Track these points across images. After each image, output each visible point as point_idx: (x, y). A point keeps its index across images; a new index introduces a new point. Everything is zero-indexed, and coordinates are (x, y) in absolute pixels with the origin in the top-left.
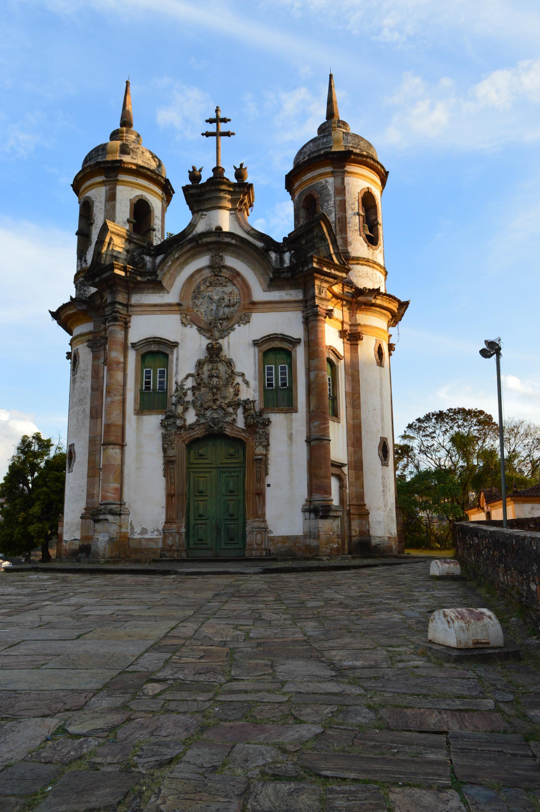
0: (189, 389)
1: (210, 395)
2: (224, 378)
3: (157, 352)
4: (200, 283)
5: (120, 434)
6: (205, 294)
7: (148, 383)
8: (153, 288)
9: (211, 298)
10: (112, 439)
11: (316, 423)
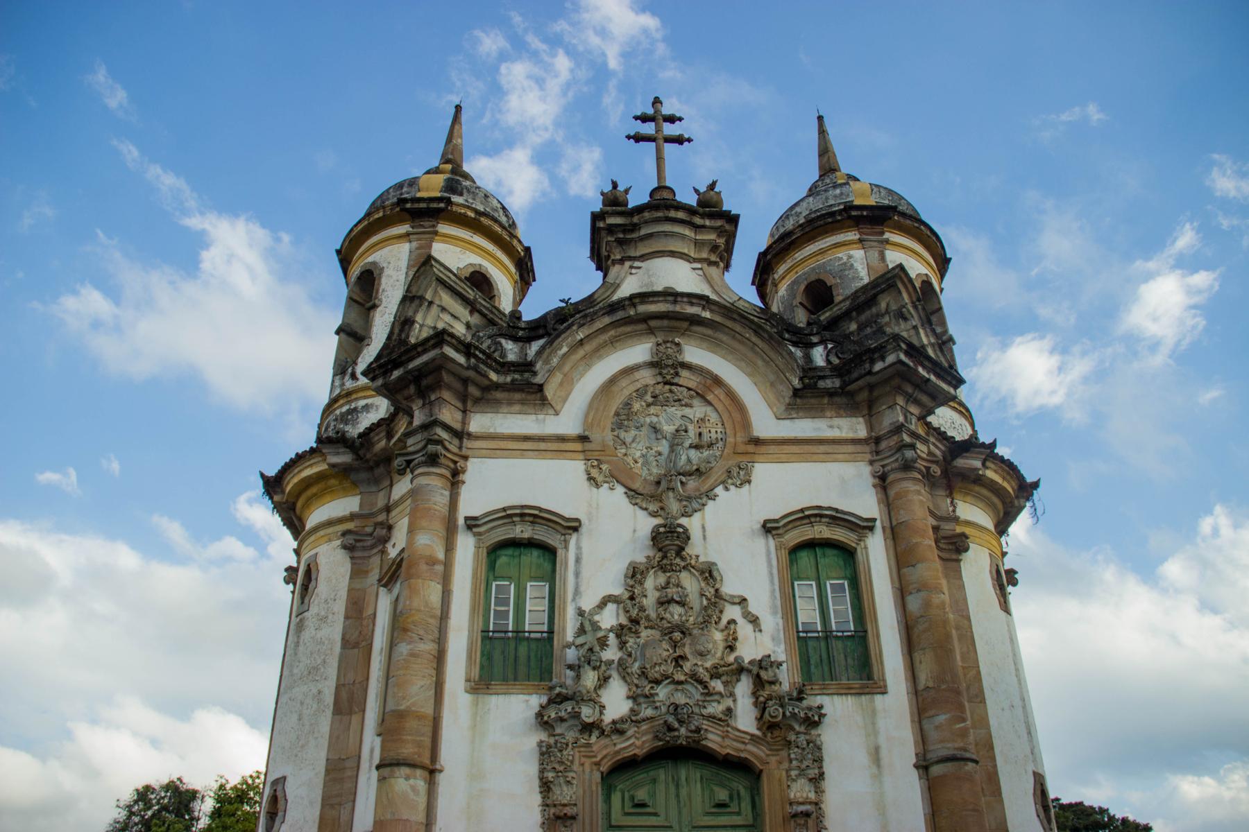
0: (611, 630)
1: (665, 645)
2: (697, 607)
3: (528, 542)
4: (630, 397)
5: (427, 741)
6: (642, 420)
8: (522, 402)
9: (655, 429)
10: (407, 751)
11: (942, 718)
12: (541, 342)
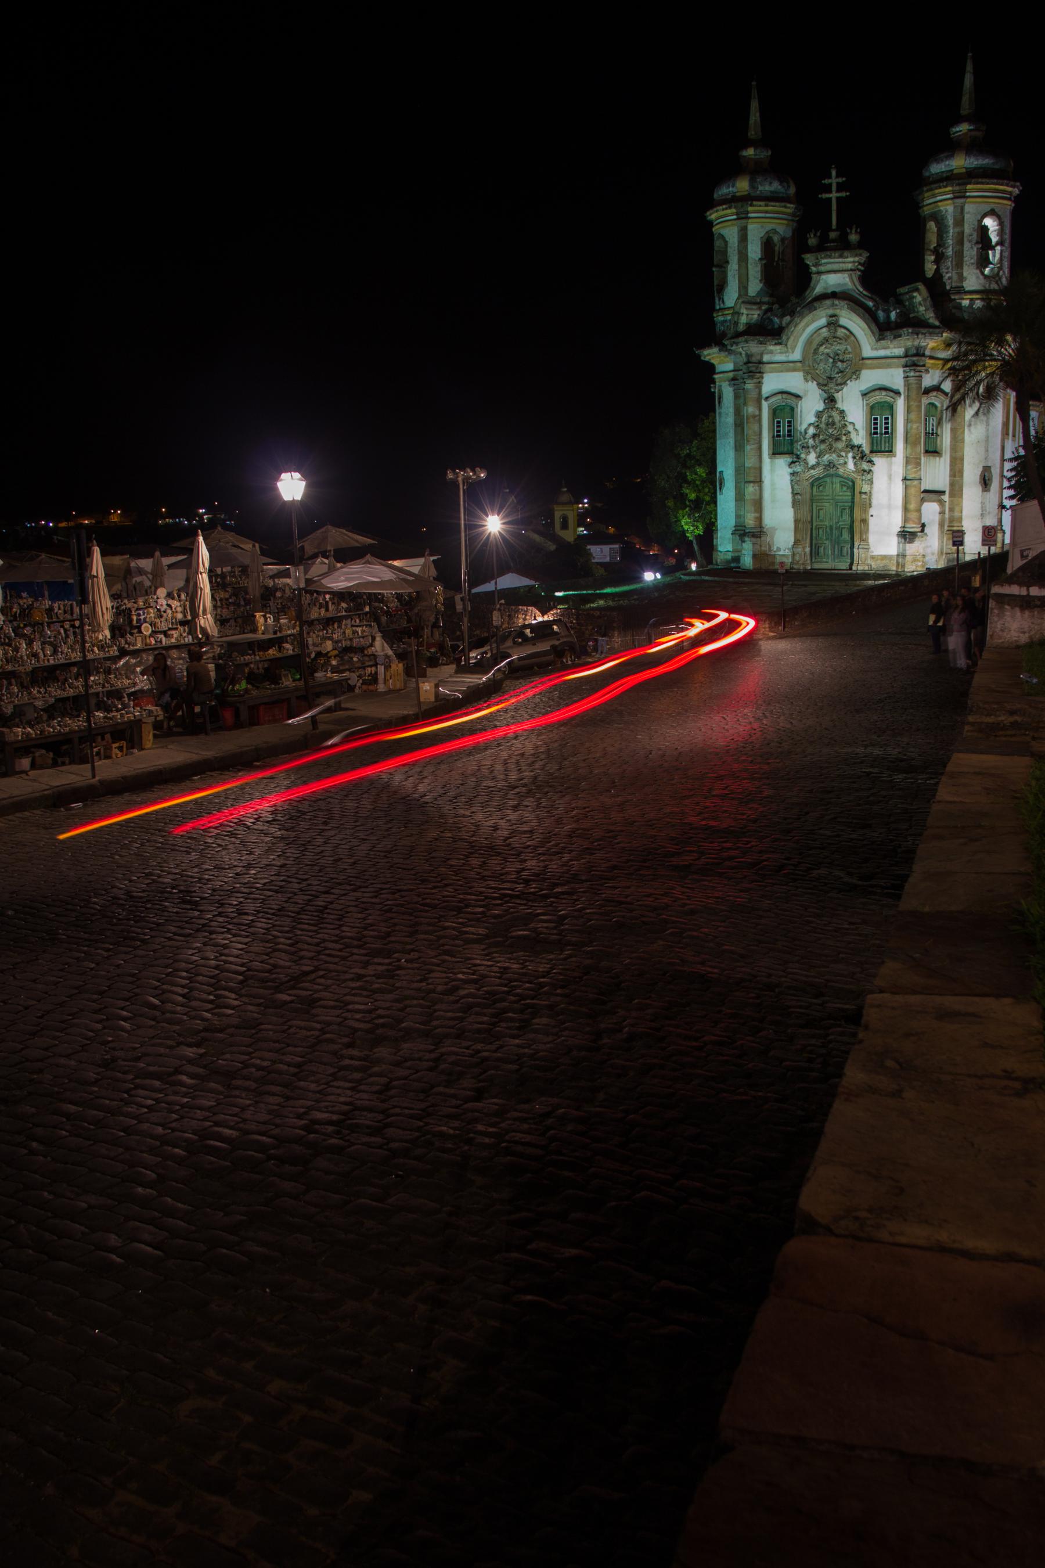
7: (778, 431)
12: (788, 318)
